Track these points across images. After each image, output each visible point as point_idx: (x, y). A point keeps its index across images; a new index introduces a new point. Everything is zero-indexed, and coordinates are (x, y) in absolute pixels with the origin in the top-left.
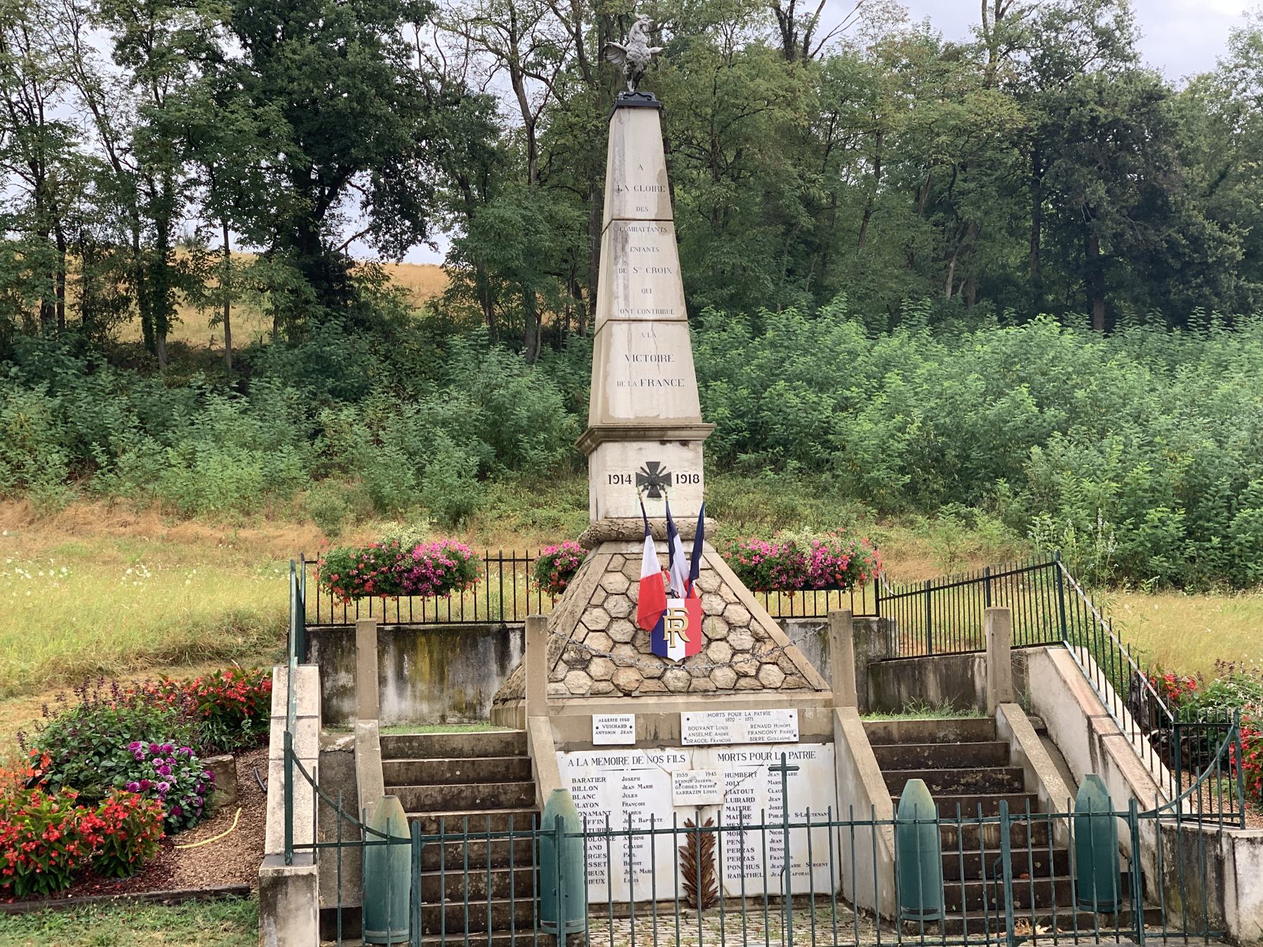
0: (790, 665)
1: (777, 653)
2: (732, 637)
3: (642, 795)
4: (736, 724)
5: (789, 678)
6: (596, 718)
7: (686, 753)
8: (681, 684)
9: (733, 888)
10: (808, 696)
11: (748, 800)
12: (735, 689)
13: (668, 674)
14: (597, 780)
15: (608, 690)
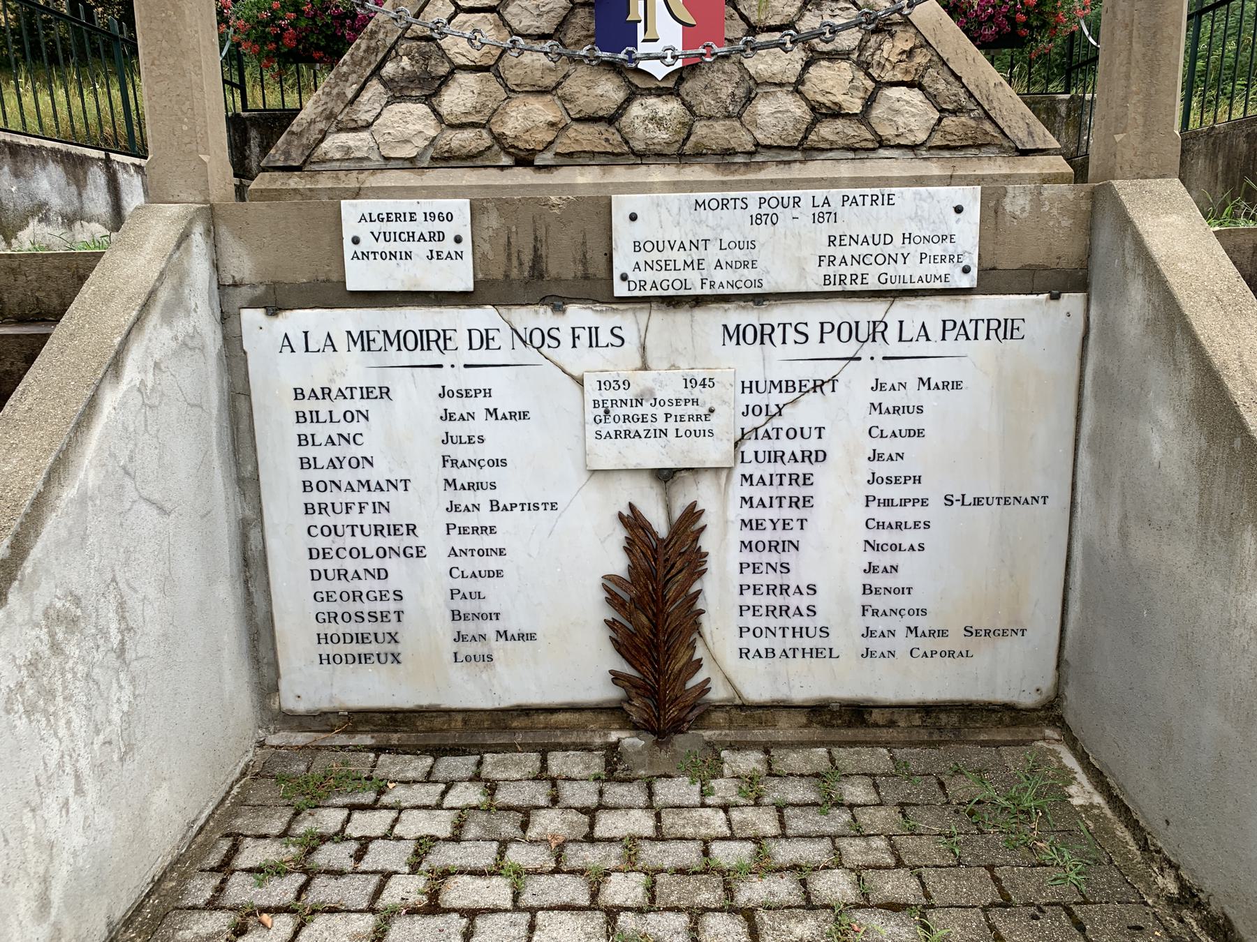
0: (956, 88)
1: (921, 58)
4: (788, 235)
5: (949, 121)
6: (350, 210)
7: (628, 322)
8: (663, 136)
9: (758, 684)
10: (996, 166)
11: (807, 456)
12: (805, 148)
13: (636, 110)
14: (367, 393)
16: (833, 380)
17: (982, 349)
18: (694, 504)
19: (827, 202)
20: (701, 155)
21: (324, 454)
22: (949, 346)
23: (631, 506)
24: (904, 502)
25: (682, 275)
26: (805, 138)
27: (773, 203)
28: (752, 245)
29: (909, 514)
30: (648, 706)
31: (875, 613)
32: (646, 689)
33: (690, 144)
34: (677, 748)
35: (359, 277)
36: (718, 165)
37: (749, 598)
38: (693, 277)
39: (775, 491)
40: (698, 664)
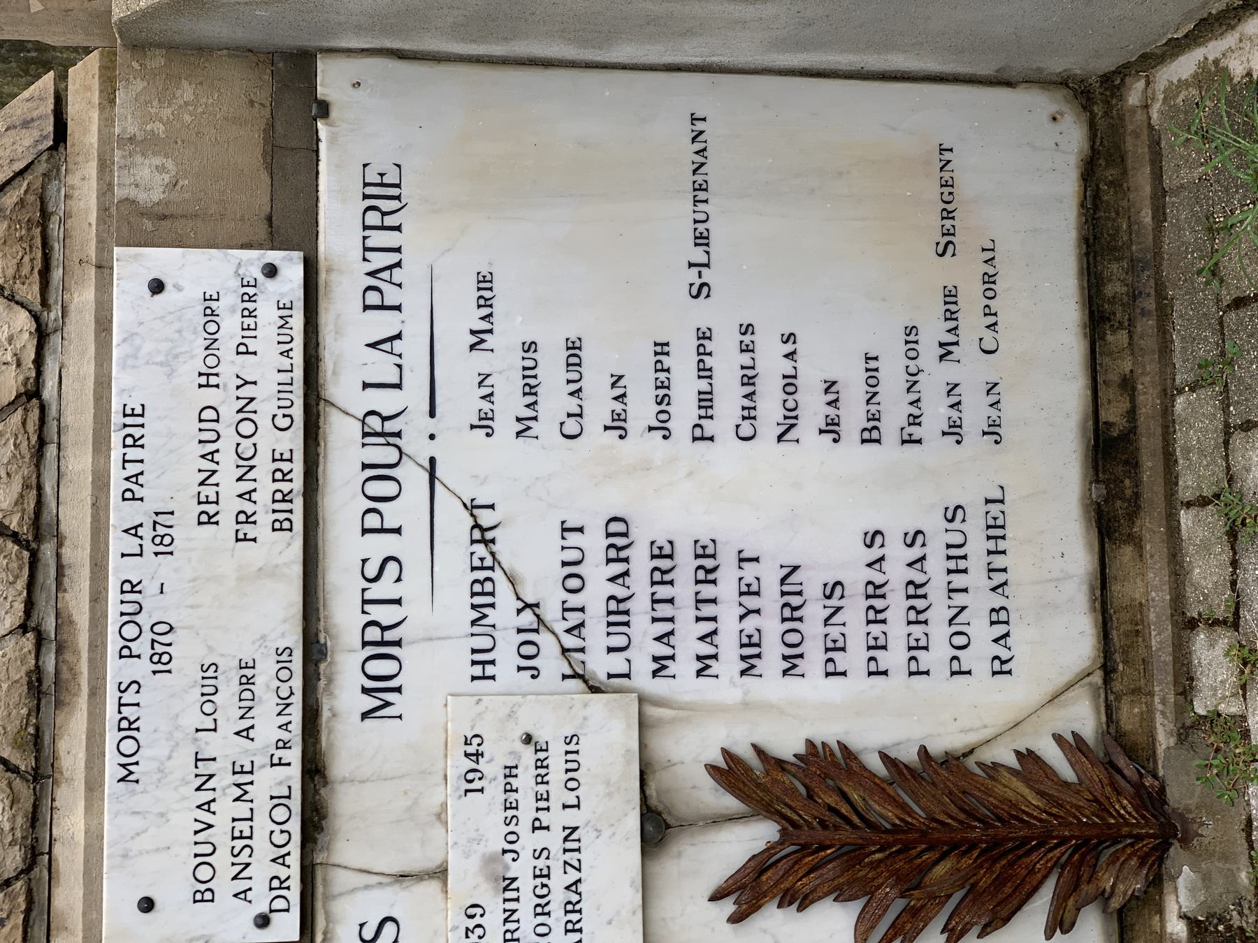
9: (1060, 639)
10: (82, 192)
11: (617, 553)
16: (472, 507)
17: (418, 238)
18: (712, 769)
19: (133, 531)
20: (37, 737)
22: (412, 297)
23: (716, 897)
24: (705, 372)
25: (262, 804)
26: (15, 537)
27: (130, 631)
28: (209, 670)
29: (726, 363)
30: (1113, 860)
31: (915, 420)
32: (1081, 861)
33: (16, 759)
34: (1192, 802)
36: (59, 704)
37: (895, 658)
38: (267, 782)
39: (685, 613)
40: (1028, 757)
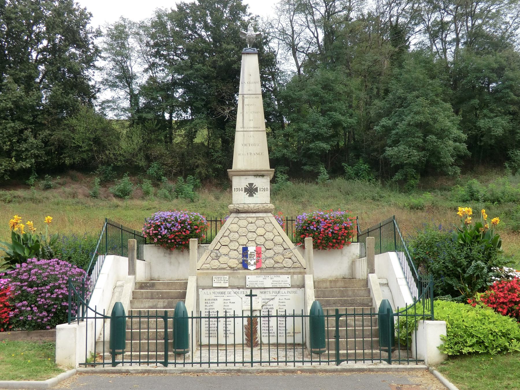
2: (275, 248)
3: (231, 306)
15: (225, 267)
21: (208, 308)
35: (215, 285)
